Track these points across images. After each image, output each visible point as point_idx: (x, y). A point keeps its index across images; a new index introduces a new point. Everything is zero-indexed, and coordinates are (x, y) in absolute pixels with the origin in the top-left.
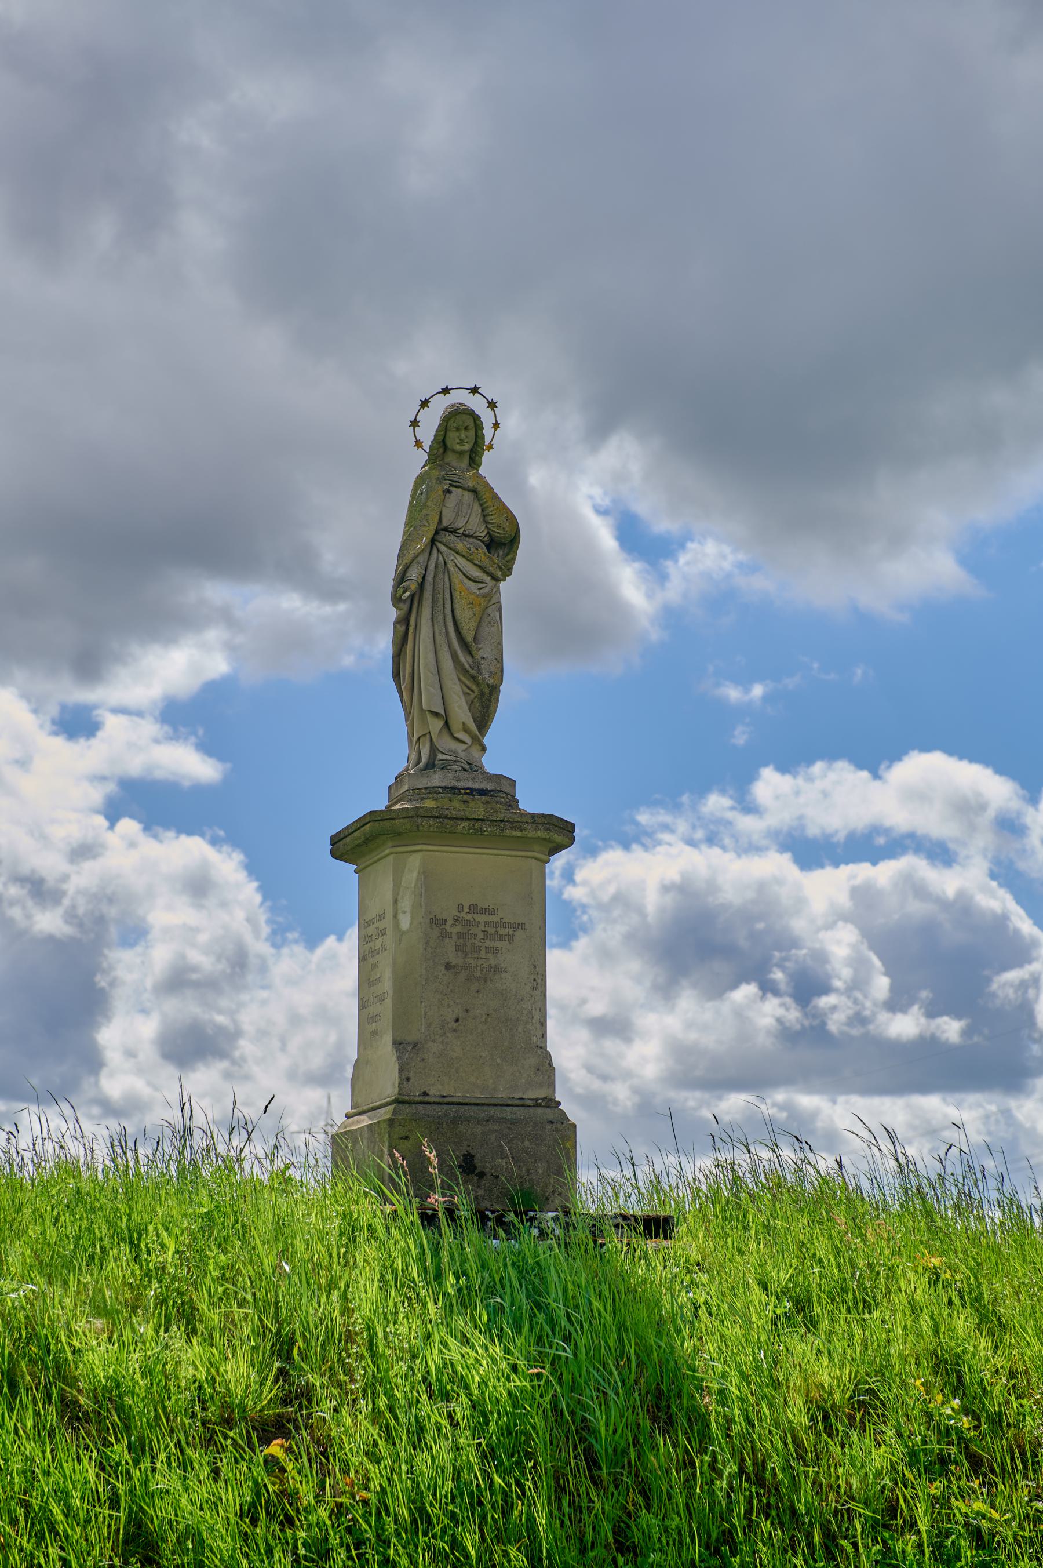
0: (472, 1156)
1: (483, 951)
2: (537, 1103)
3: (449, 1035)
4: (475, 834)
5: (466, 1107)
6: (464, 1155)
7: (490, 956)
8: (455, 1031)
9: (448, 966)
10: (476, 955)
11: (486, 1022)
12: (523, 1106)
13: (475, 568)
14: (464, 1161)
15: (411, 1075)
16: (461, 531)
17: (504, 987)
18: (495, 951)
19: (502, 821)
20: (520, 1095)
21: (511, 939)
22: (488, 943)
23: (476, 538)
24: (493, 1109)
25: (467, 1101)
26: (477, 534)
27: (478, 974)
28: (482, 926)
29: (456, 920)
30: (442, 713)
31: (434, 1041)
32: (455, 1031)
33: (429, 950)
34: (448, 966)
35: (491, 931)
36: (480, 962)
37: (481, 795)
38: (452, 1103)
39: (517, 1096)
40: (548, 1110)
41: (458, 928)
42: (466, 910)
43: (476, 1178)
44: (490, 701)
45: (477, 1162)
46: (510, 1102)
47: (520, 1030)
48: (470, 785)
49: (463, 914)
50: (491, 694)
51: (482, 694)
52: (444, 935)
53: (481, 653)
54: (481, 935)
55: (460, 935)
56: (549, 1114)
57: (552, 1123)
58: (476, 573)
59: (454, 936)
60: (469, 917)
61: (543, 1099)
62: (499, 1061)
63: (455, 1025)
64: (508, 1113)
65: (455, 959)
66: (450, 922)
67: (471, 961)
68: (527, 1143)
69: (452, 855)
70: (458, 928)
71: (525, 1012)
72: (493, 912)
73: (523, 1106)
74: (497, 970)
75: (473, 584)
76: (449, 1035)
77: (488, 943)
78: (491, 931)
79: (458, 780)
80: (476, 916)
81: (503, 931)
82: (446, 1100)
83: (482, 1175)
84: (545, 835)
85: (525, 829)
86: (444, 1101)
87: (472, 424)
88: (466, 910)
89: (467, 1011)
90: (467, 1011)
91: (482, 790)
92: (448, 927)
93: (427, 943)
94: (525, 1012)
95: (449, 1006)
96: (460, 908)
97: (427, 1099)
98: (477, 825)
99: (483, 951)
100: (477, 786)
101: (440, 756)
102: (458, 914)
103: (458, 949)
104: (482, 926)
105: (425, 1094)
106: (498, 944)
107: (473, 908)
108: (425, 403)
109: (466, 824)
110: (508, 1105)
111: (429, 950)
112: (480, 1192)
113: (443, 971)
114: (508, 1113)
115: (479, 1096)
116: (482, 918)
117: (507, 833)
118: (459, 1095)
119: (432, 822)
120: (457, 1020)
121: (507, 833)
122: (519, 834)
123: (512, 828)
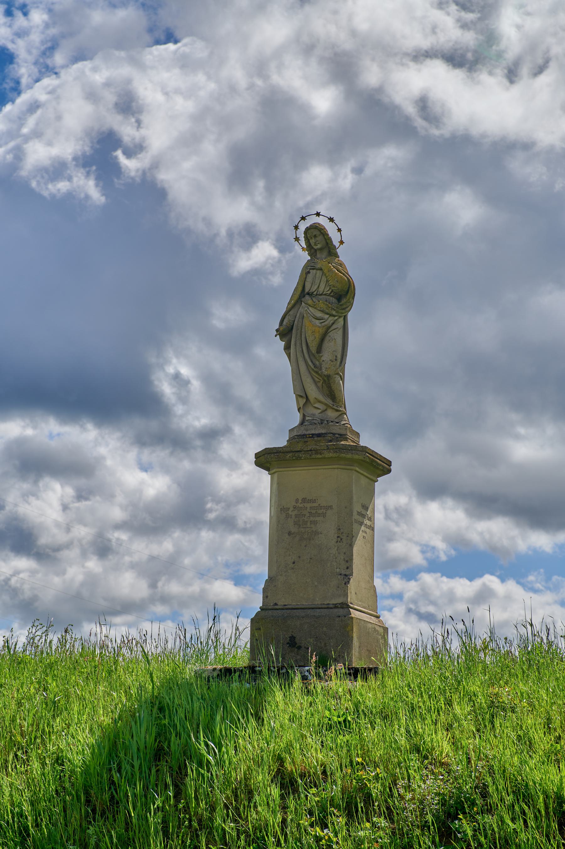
0: (295, 638)
1: (309, 524)
2: (336, 606)
3: (289, 571)
4: (297, 459)
5: (295, 611)
6: (290, 637)
7: (312, 526)
8: (293, 569)
9: (290, 533)
10: (305, 526)
11: (310, 562)
12: (328, 608)
13: (319, 312)
14: (290, 640)
15: (269, 594)
16: (315, 293)
17: (320, 542)
18: (315, 523)
19: (311, 450)
20: (328, 602)
21: (324, 515)
22: (312, 519)
23: (325, 294)
24: (309, 611)
25: (297, 607)
26: (324, 293)
27: (306, 536)
28: (308, 509)
29: (295, 507)
30: (304, 396)
31: (281, 575)
32: (293, 569)
33: (280, 525)
34: (290, 533)
35: (314, 512)
36: (307, 529)
37: (318, 437)
38: (289, 609)
39: (325, 603)
40: (341, 610)
41: (296, 512)
42: (300, 501)
43: (296, 650)
44: (330, 384)
45: (297, 640)
46: (320, 606)
47: (329, 565)
48: (313, 432)
49: (298, 504)
50: (329, 380)
51: (324, 381)
52: (288, 516)
53: (323, 358)
54: (308, 515)
55: (296, 516)
56: (341, 612)
57: (339, 617)
58: (319, 314)
59: (293, 517)
60: (301, 505)
61: (340, 604)
62: (316, 583)
63: (292, 565)
64: (317, 612)
65: (294, 529)
66: (292, 509)
67: (302, 529)
68: (325, 629)
69: (293, 472)
70: (296, 512)
71: (332, 555)
72: (314, 501)
73: (328, 608)
74: (317, 533)
75: (317, 321)
76: (289, 571)
77: (312, 519)
78: (314, 512)
79: (307, 430)
80: (305, 504)
81: (320, 511)
82: (287, 607)
83: (299, 648)
84: (335, 455)
85: (323, 453)
86: (285, 608)
87: (317, 233)
88: (300, 501)
89: (299, 557)
90: (299, 557)
91: (319, 434)
92: (290, 513)
93: (279, 522)
94: (332, 555)
95: (289, 555)
96: (297, 501)
97: (276, 607)
98: (297, 454)
99: (309, 524)
100: (317, 432)
101: (307, 418)
102: (296, 504)
103: (295, 523)
104: (308, 509)
105: (276, 604)
106: (317, 519)
107: (304, 500)
108: (339, 230)
109: (290, 455)
110: (319, 608)
111: (280, 525)
112: (299, 657)
113: (287, 536)
114: (317, 612)
115: (305, 603)
116: (308, 505)
117: (313, 456)
118: (294, 604)
119: (272, 456)
120: (294, 563)
121: (313, 456)
122: (320, 456)
123: (315, 454)
